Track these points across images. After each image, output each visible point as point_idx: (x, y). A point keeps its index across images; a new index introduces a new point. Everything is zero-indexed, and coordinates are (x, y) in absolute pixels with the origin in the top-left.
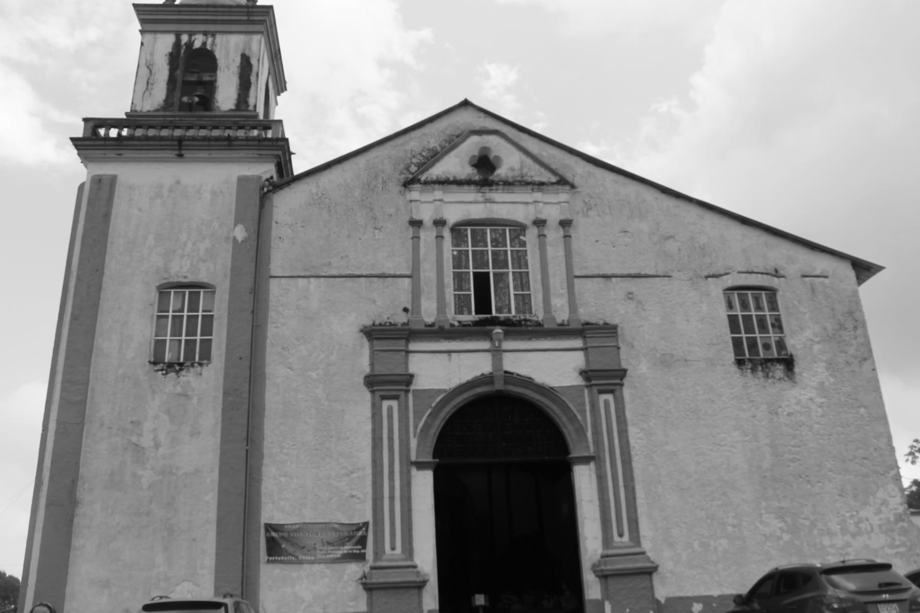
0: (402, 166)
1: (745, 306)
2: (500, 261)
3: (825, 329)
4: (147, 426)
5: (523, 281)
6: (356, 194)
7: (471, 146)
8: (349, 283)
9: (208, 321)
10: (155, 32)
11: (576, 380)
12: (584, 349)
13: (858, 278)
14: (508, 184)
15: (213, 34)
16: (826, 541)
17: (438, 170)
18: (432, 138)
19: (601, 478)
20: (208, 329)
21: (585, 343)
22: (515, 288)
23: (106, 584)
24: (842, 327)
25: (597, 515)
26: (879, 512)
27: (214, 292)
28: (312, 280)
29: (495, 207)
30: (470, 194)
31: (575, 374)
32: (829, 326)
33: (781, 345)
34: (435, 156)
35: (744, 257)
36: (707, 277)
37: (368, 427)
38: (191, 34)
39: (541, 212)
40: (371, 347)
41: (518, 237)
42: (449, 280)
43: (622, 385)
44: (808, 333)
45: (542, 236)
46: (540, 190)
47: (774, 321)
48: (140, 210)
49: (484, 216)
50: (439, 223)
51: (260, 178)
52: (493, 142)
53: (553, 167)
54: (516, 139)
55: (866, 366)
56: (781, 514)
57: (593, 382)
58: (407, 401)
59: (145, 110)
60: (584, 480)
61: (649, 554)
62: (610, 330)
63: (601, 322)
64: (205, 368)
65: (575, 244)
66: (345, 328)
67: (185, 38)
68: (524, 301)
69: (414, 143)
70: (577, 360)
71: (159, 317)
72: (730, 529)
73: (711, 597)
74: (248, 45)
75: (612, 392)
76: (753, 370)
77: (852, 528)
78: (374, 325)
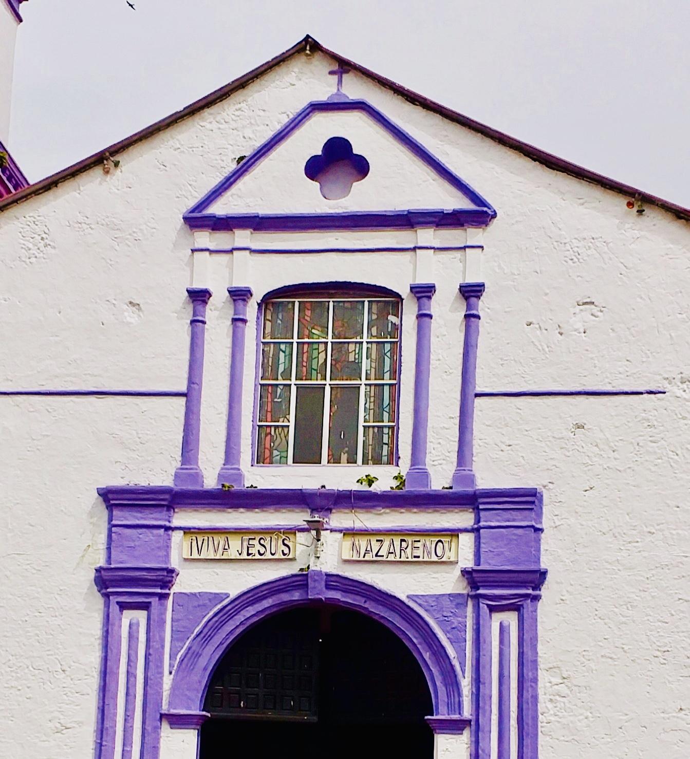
21: (478, 520)
43: (536, 598)
45: (423, 317)
57: (481, 591)
58: (163, 613)
75: (517, 608)
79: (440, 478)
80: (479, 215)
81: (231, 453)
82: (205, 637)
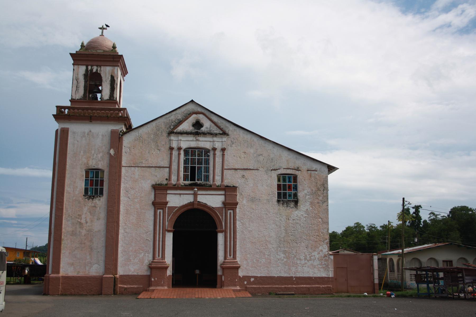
0: (168, 126)
1: (284, 181)
2: (200, 162)
3: (312, 190)
4: (83, 216)
5: (207, 170)
6: (152, 137)
7: (192, 119)
8: (148, 169)
9: (102, 182)
10: (78, 65)
12: (225, 195)
13: (329, 171)
14: (204, 134)
15: (100, 66)
16: (298, 262)
17: (180, 128)
18: (179, 115)
20: (102, 184)
21: (225, 193)
22: (204, 172)
23: (72, 264)
24: (318, 189)
25: (223, 249)
26: (319, 253)
27: (104, 172)
28: (136, 168)
29: (200, 143)
30: (191, 138)
31: (221, 203)
32: (314, 189)
33: (296, 195)
34: (180, 122)
35: (286, 163)
36: (272, 170)
37: (152, 218)
38: (92, 66)
39: (215, 145)
40: (155, 192)
41: (207, 153)
42: (182, 169)
44: (306, 192)
45: (214, 154)
46: (216, 137)
48: (78, 141)
49: (195, 146)
50: (179, 149)
51: (118, 130)
52: (201, 117)
53: (222, 127)
54: (209, 116)
55: (325, 204)
56: (285, 252)
59: (76, 99)
60: (221, 237)
61: (239, 262)
62: (234, 188)
63: (232, 186)
64: (101, 198)
65: (226, 157)
66: (147, 185)
67: (90, 68)
68: (207, 178)
69: (173, 117)
70: (222, 198)
71: (86, 180)
72: (267, 256)
73: (257, 277)
74: (113, 71)
76: (283, 204)
77: (308, 258)
78: (156, 184)
81: (178, 180)
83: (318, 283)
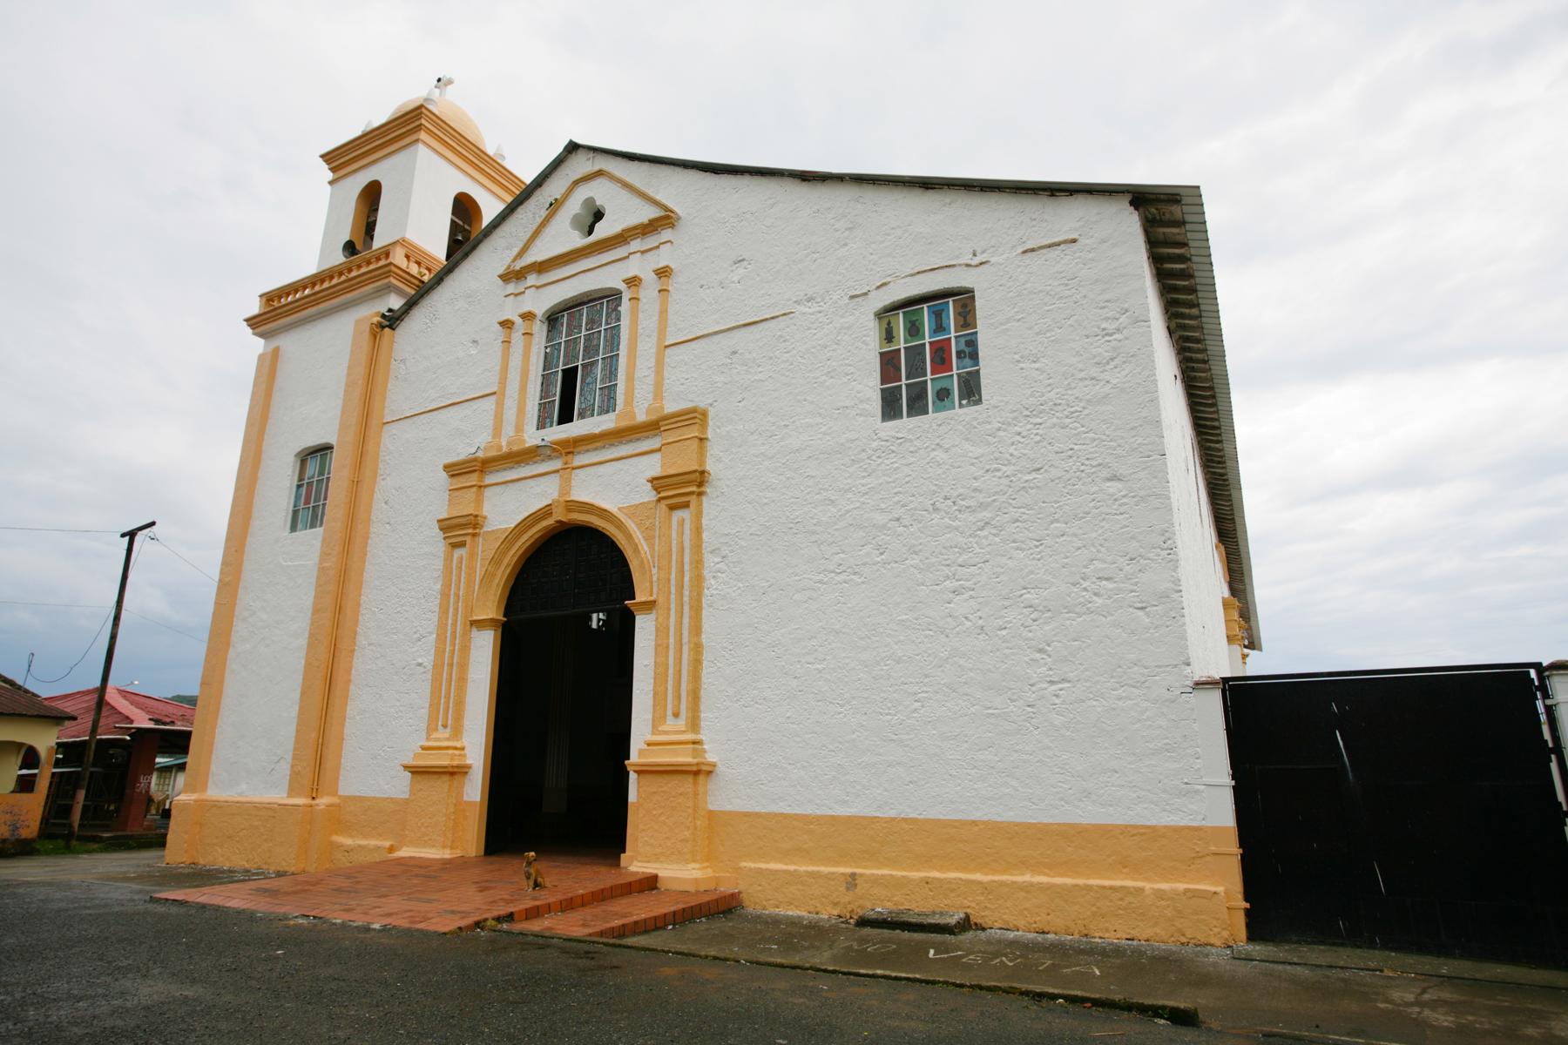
1: (914, 330)
2: (591, 349)
7: (574, 206)
11: (647, 495)
19: (662, 631)
22: (602, 381)
47: (962, 346)
50: (528, 316)
79: (641, 417)
80: (666, 220)
81: (519, 428)
82: (495, 561)
83: (1124, 864)
